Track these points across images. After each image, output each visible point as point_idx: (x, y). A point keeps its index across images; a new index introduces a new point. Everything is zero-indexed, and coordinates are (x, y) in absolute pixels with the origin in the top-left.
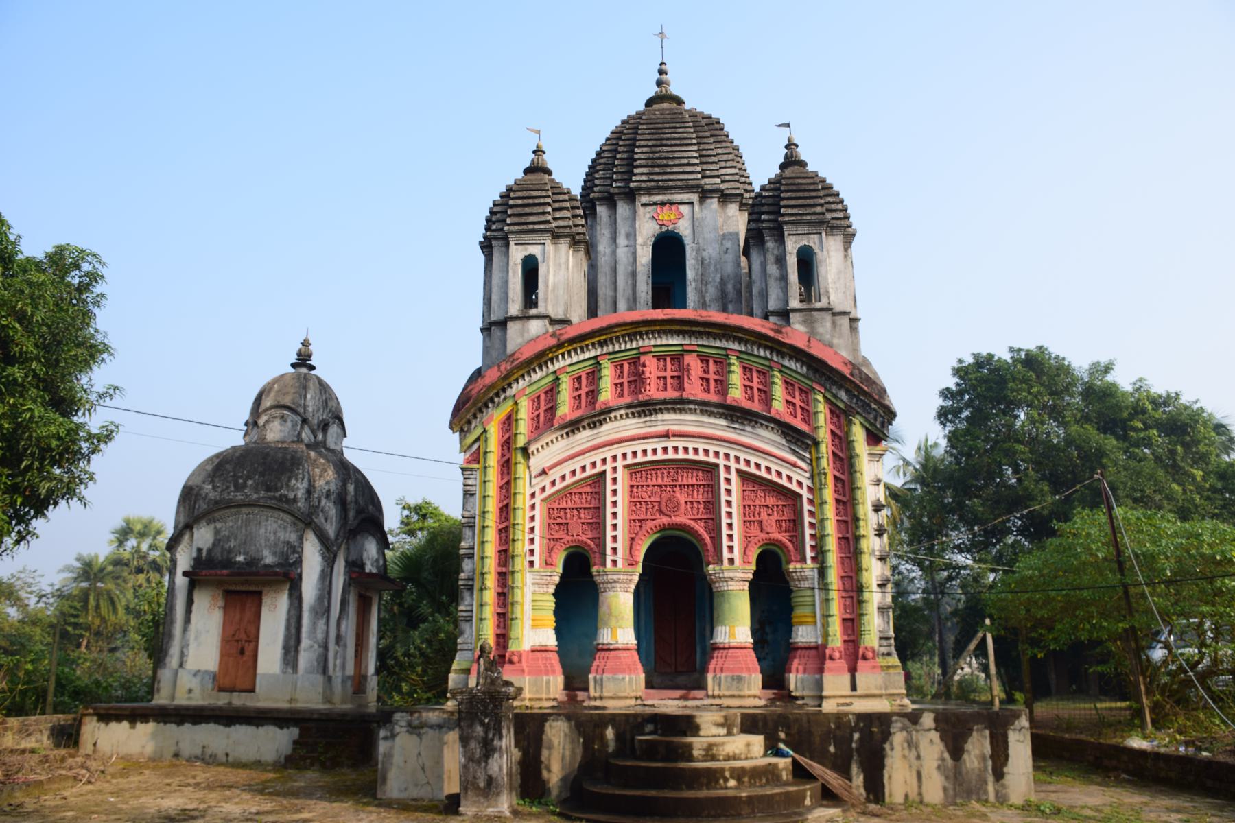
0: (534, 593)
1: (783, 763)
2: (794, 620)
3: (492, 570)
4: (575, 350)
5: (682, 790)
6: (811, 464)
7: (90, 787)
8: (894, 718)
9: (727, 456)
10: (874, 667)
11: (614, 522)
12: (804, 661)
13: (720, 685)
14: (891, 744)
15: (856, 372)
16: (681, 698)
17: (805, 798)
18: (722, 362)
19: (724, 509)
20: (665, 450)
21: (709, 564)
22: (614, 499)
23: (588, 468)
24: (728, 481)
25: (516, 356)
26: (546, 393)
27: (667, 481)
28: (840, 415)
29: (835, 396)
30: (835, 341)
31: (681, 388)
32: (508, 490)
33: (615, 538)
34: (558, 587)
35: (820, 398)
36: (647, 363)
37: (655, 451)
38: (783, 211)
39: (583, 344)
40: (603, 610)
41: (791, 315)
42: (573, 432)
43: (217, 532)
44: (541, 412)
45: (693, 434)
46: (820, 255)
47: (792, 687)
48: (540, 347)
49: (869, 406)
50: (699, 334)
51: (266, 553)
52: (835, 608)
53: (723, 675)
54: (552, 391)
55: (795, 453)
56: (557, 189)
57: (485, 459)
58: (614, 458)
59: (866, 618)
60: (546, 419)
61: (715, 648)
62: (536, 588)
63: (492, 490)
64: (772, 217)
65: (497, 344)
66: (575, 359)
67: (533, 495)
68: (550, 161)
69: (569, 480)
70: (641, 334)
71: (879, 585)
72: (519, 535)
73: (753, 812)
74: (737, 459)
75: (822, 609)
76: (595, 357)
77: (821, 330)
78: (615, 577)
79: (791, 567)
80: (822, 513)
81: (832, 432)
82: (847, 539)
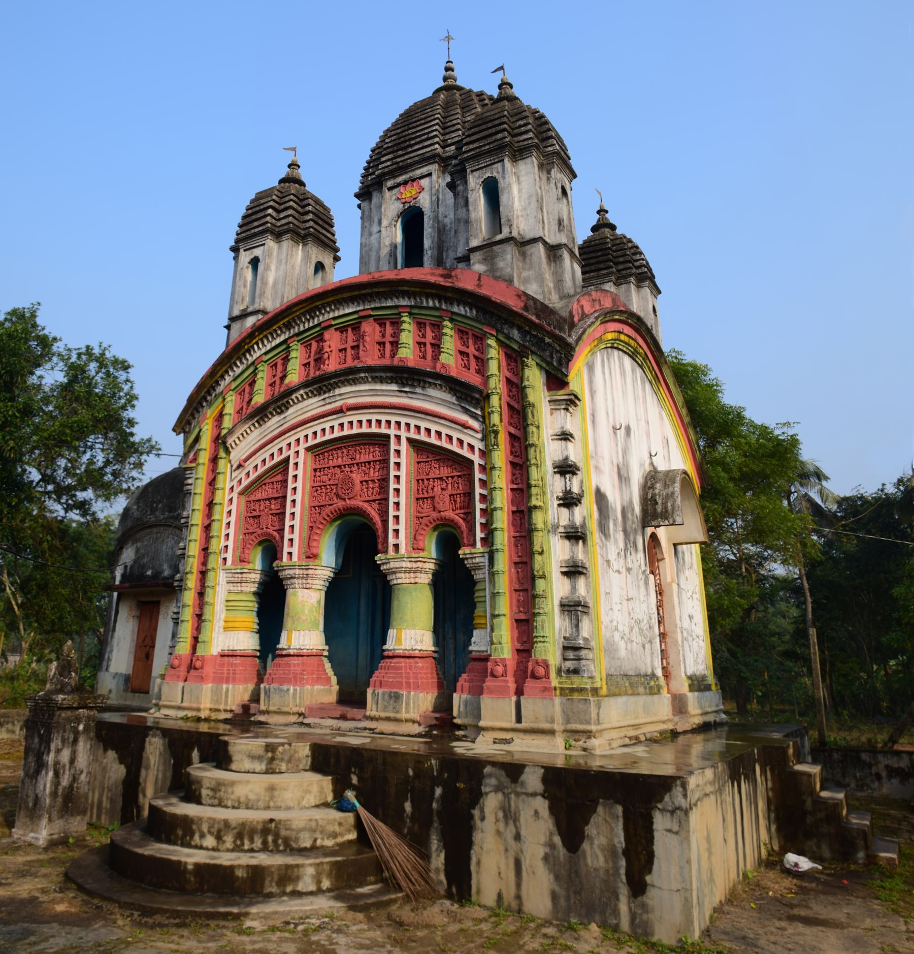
3: (195, 570)
28: (514, 360)
31: (357, 357)
43: (137, 550)
45: (366, 406)
51: (165, 566)
55: (466, 411)
59: (539, 619)
62: (231, 587)
67: (232, 489)
69: (261, 470)
77: (501, 264)
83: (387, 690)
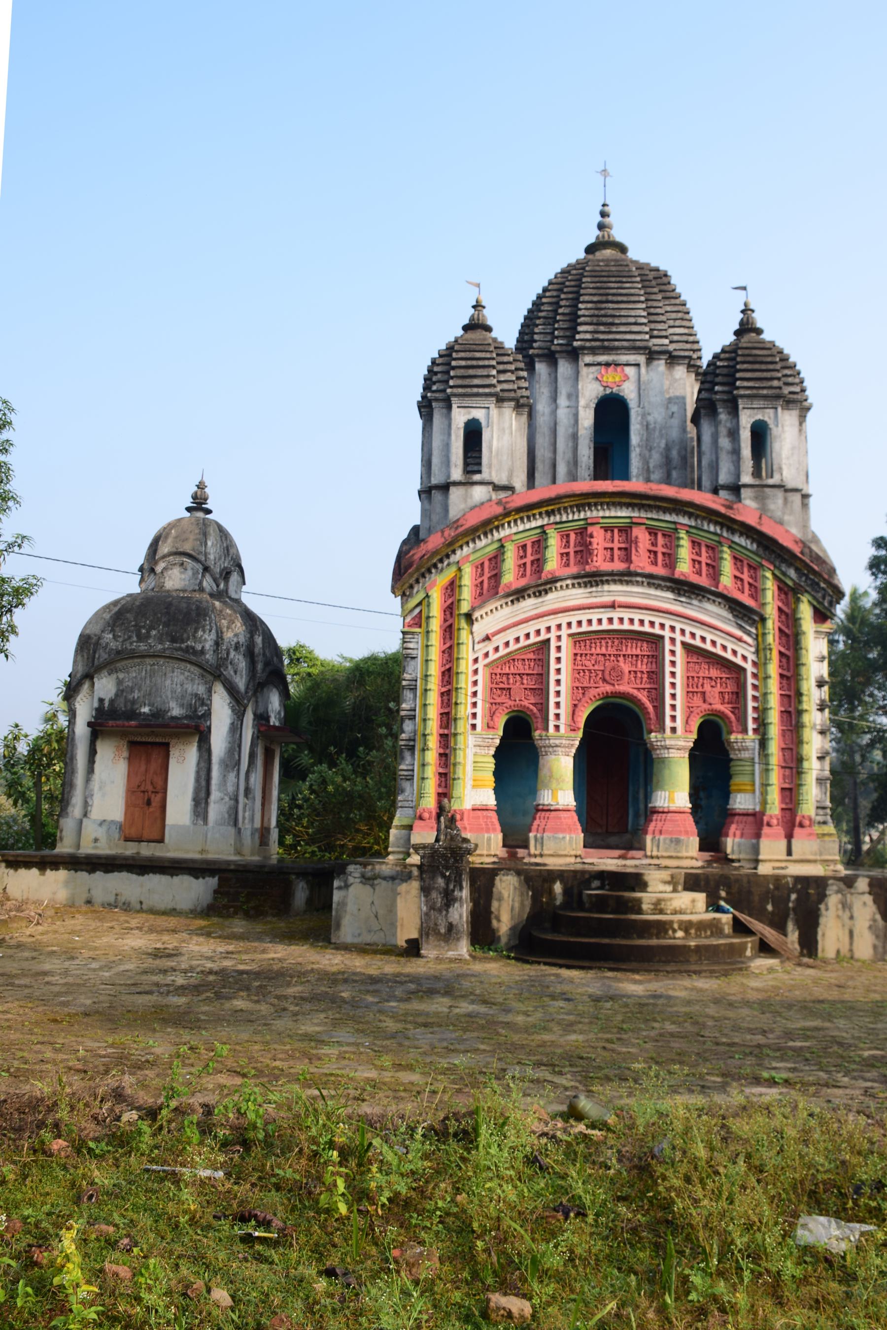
0: (475, 754)
1: (726, 919)
2: (732, 788)
4: (522, 519)
6: (756, 639)
7: (40, 928)
8: (830, 882)
9: (673, 629)
10: (810, 834)
11: (558, 689)
12: (741, 826)
13: (658, 847)
15: (807, 551)
16: (620, 857)
17: (746, 949)
18: (671, 536)
19: (668, 679)
20: (610, 620)
21: (651, 732)
22: (558, 666)
23: (532, 636)
24: (673, 653)
25: (460, 523)
26: (490, 560)
28: (788, 593)
29: (784, 574)
30: (786, 518)
31: (628, 559)
32: (450, 655)
33: (558, 705)
34: (498, 749)
35: (769, 575)
36: (595, 534)
37: (600, 621)
38: (738, 383)
39: (530, 513)
40: (543, 773)
41: (743, 491)
42: (518, 600)
44: (485, 578)
45: (638, 606)
46: (775, 431)
47: (729, 850)
48: (485, 515)
49: (818, 584)
50: (649, 508)
52: (775, 778)
53: (662, 837)
54: (497, 558)
55: (741, 627)
56: (499, 347)
57: (428, 624)
58: (559, 627)
59: (804, 788)
60: (490, 586)
61: (655, 811)
62: (478, 750)
63: (435, 654)
64: (726, 388)
65: (438, 508)
66: (521, 527)
67: (476, 660)
68: (490, 317)
69: (513, 647)
70: (589, 505)
71: (819, 758)
72: (461, 699)
73: (700, 959)
74: (683, 632)
75: (761, 778)
76: (542, 527)
77: (772, 507)
78: (557, 742)
79: (733, 737)
80: (766, 686)
81: (780, 609)
82: (789, 712)
83: (669, 837)
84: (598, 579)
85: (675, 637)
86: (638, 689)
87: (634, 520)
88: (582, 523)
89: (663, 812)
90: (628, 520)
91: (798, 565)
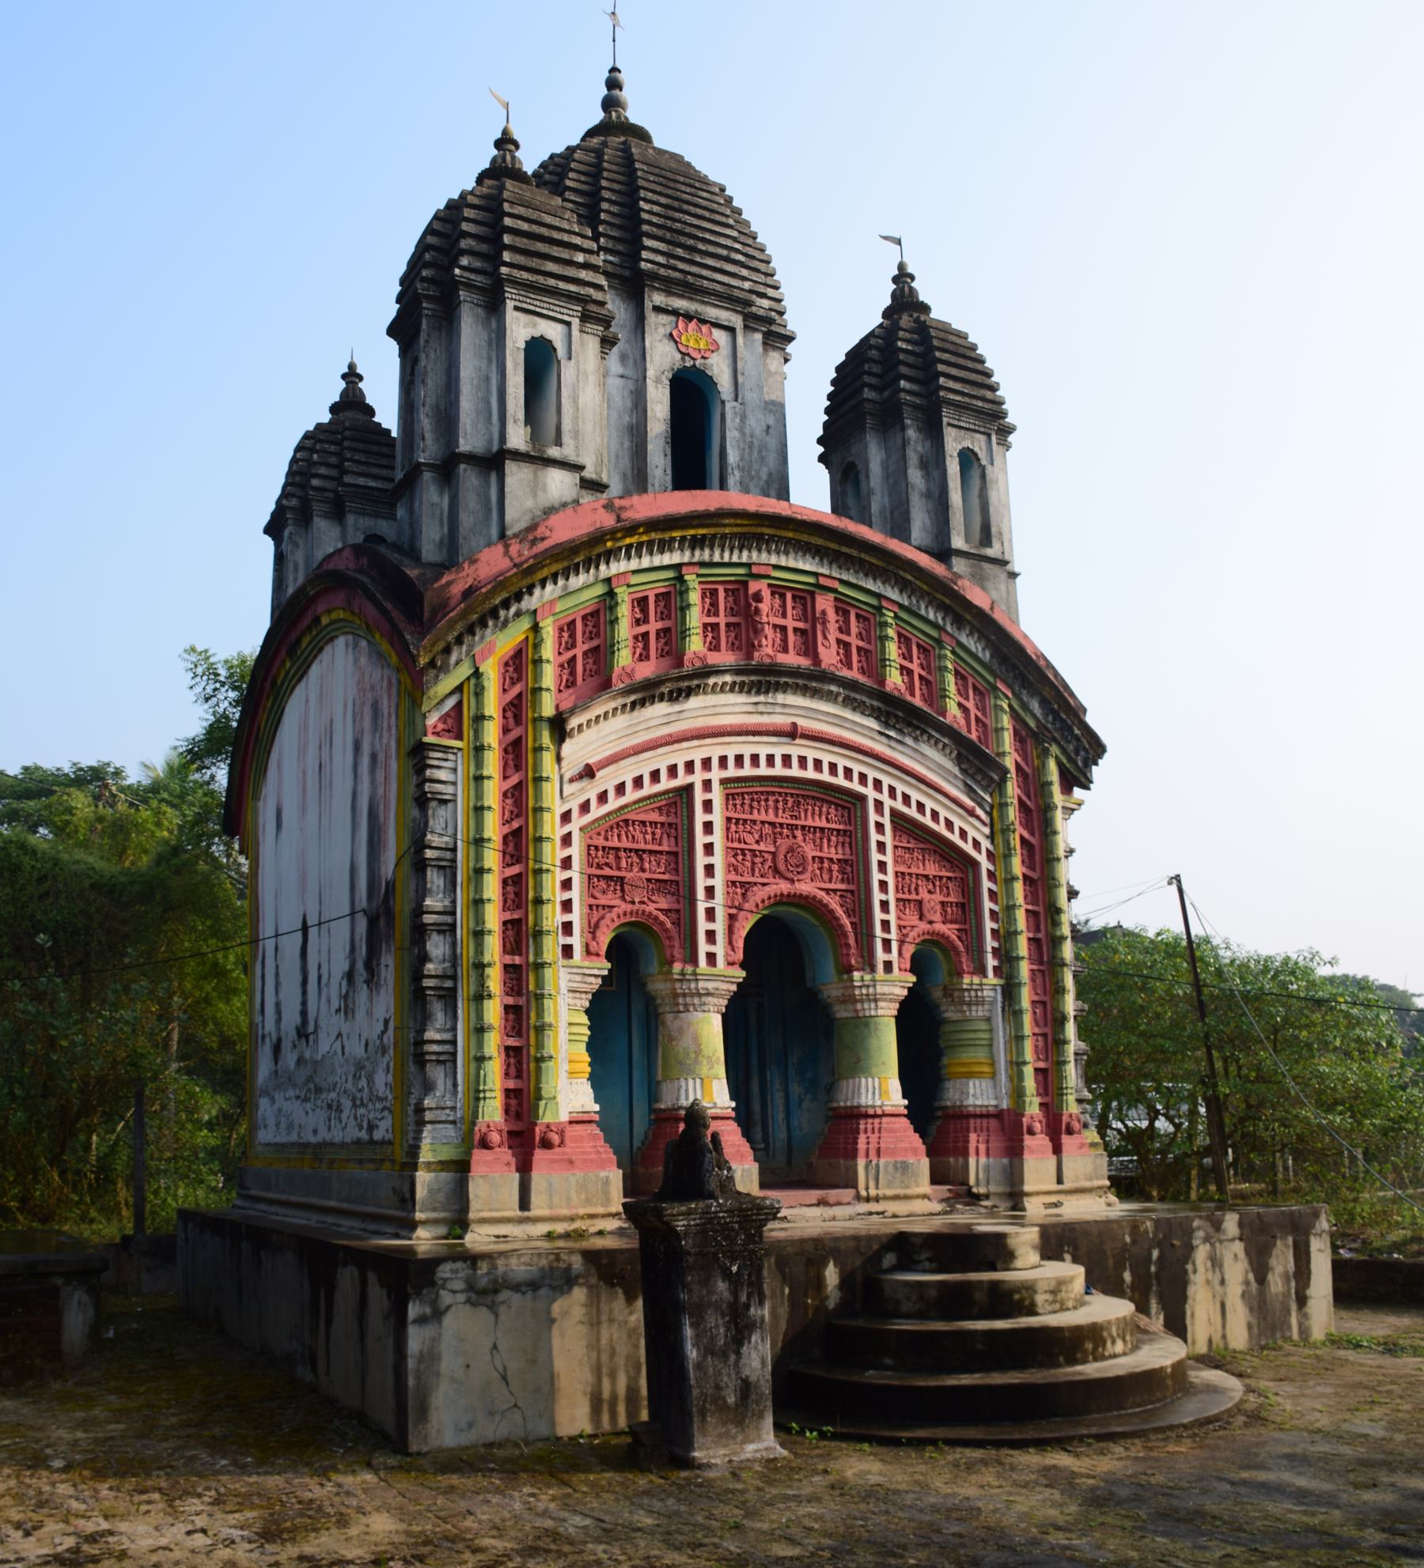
5: (1059, 1366)
6: (990, 814)
9: (878, 784)
10: (1082, 1146)
14: (1194, 1264)
18: (871, 618)
26: (584, 618)
27: (784, 818)
29: (1025, 707)
42: (642, 703)
45: (827, 739)
54: (600, 617)
55: (970, 791)
58: (707, 763)
60: (593, 673)
63: (492, 793)
66: (646, 562)
67: (566, 817)
74: (892, 791)
76: (678, 567)
78: (711, 985)
83: (891, 1160)
84: (772, 679)
85: (884, 797)
86: (827, 891)
87: (822, 581)
88: (741, 571)
89: (875, 1116)
90: (811, 580)
91: (1046, 693)
